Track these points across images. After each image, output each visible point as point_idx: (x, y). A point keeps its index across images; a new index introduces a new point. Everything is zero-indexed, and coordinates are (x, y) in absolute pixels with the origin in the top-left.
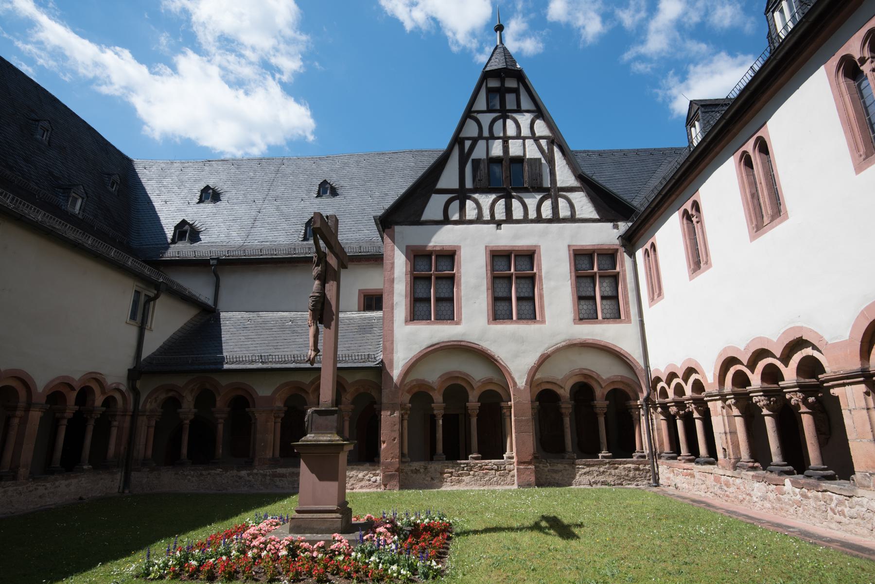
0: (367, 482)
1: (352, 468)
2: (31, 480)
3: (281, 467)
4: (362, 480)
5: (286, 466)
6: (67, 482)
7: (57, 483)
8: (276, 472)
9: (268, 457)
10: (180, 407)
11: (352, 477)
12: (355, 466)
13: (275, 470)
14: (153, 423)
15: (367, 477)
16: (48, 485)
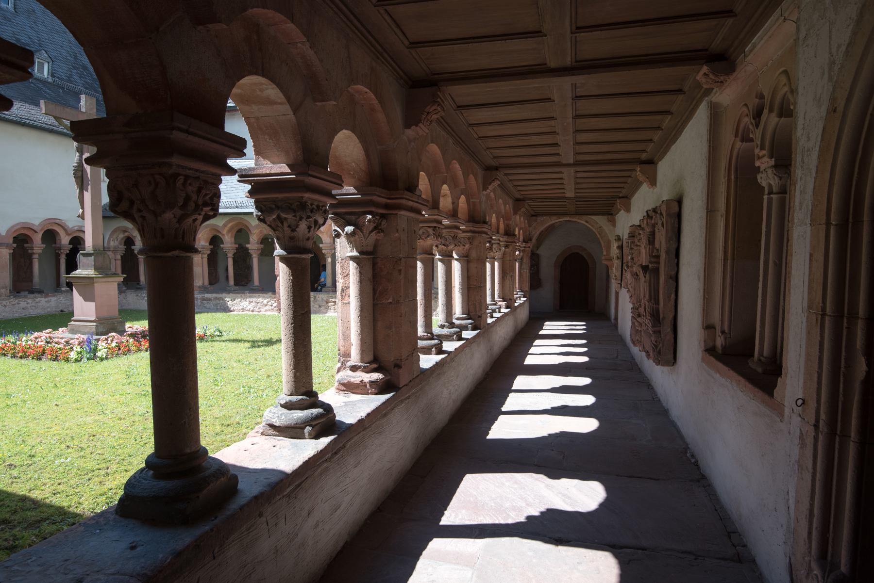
0: (270, 307)
1: (259, 296)
2: (12, 297)
3: (207, 293)
4: (266, 305)
5: (211, 293)
6: (47, 299)
7: (37, 300)
8: (204, 296)
9: (198, 285)
10: (134, 245)
11: (259, 302)
12: (261, 294)
13: (203, 295)
14: (119, 257)
15: (270, 303)
16: (29, 301)
